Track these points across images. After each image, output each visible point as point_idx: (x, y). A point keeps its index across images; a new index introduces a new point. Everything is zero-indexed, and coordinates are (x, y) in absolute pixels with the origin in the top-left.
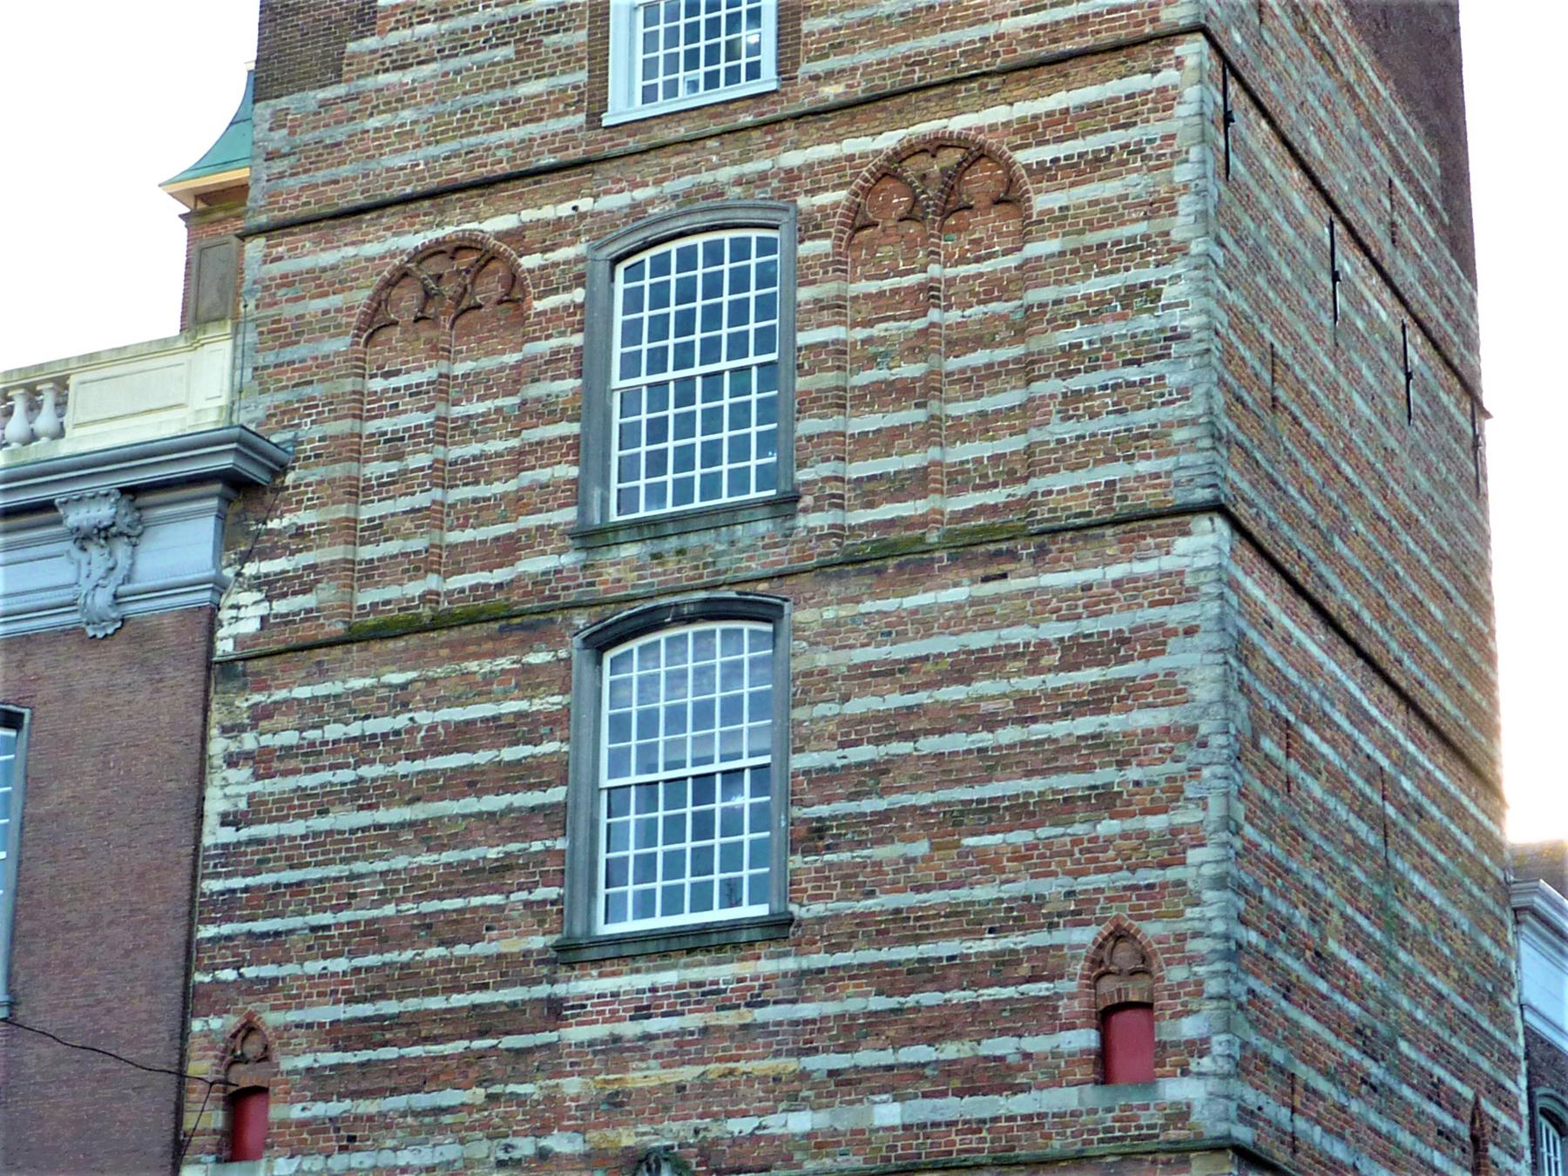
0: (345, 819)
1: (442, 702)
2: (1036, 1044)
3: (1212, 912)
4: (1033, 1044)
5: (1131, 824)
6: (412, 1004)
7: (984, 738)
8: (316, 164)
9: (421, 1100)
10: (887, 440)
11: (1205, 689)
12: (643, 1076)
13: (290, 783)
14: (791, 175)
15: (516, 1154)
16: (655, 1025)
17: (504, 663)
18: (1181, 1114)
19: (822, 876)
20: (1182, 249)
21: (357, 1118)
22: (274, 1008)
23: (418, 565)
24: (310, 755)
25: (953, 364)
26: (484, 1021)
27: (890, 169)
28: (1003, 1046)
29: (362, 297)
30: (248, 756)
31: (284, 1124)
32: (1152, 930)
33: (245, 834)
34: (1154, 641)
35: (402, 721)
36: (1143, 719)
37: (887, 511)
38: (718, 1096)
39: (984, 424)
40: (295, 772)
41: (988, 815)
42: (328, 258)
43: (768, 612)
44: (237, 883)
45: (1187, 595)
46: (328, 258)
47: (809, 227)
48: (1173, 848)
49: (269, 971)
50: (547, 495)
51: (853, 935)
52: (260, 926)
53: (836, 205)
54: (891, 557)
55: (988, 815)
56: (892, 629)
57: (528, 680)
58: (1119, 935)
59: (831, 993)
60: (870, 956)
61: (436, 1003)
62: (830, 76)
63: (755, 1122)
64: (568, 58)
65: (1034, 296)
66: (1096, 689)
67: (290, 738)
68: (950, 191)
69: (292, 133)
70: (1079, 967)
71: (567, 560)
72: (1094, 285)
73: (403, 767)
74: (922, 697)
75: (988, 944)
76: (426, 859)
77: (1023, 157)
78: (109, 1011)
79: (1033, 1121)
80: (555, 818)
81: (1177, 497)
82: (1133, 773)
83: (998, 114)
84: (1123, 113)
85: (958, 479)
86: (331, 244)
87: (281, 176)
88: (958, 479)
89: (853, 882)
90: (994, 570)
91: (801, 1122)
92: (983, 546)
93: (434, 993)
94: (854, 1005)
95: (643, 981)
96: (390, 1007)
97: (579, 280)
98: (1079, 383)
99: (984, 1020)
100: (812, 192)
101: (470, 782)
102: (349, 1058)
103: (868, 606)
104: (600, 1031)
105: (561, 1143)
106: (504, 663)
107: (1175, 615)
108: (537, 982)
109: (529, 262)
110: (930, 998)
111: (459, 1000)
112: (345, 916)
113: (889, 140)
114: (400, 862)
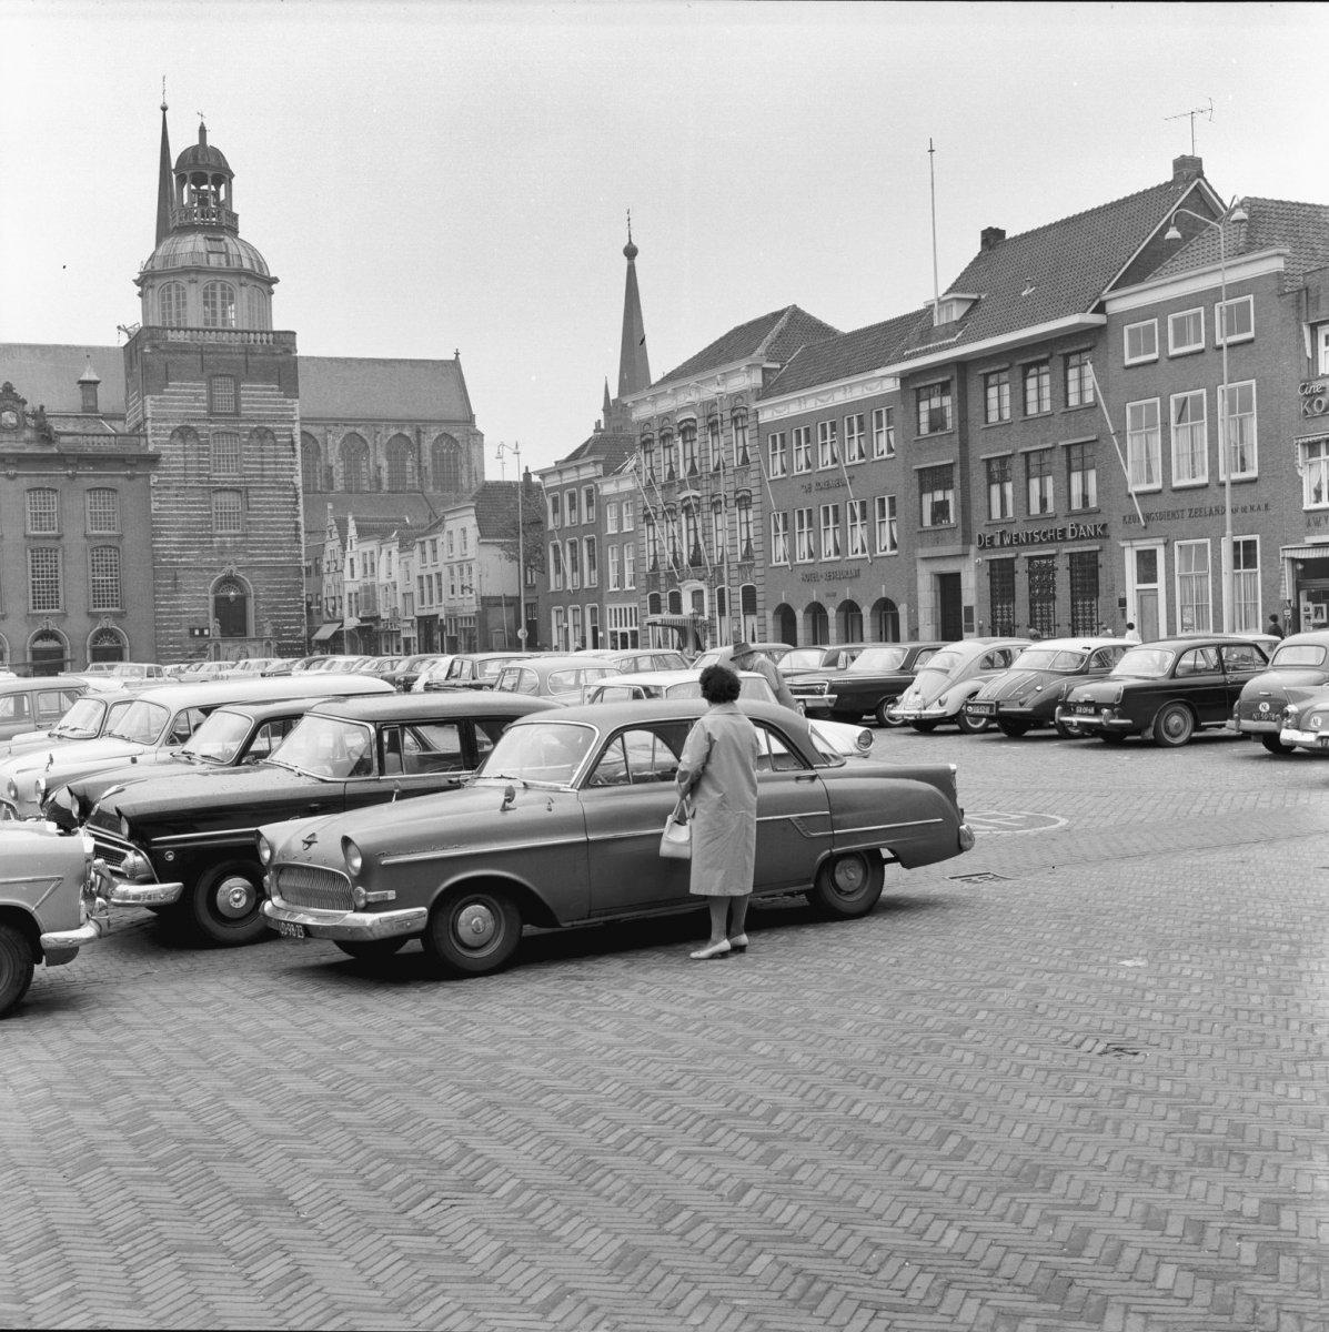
0: (175, 512)
27: (255, 430)
39: (270, 469)
47: (245, 436)
101: (195, 509)
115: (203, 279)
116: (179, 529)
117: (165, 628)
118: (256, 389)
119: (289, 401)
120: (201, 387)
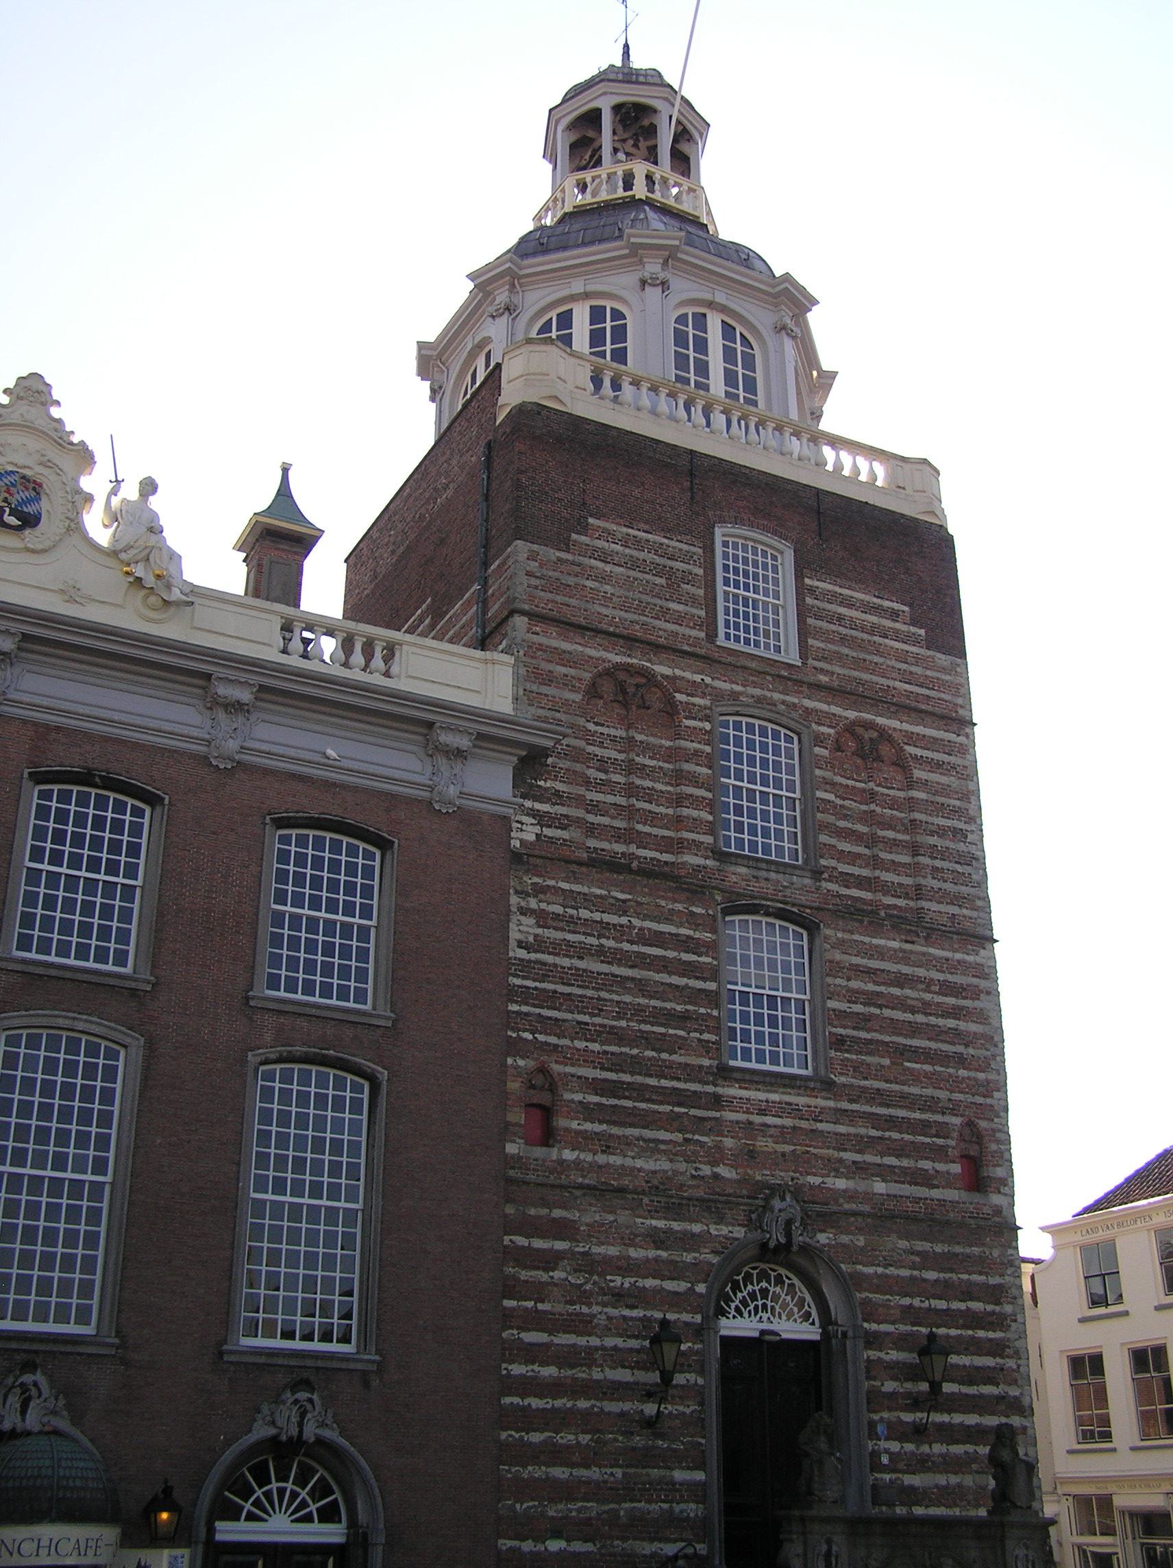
5: (972, 1074)
6: (639, 1079)
7: (909, 1016)
8: (556, 590)
9: (647, 1133)
10: (853, 858)
12: (764, 1144)
13: (559, 935)
14: (808, 711)
15: (701, 1173)
16: (770, 1120)
17: (679, 907)
21: (610, 1135)
22: (557, 1062)
23: (619, 835)
24: (572, 924)
28: (926, 1165)
30: (533, 912)
31: (567, 1130)
32: (983, 1124)
33: (533, 956)
35: (624, 920)
36: (973, 1028)
38: (802, 1162)
40: (563, 930)
42: (565, 646)
46: (565, 646)
49: (552, 1040)
51: (860, 1097)
52: (546, 1012)
53: (829, 735)
57: (692, 920)
58: (970, 1124)
59: (852, 1123)
60: (867, 1108)
61: (652, 1082)
63: (821, 1180)
64: (693, 600)
65: (917, 816)
66: (954, 1007)
67: (558, 909)
69: (541, 566)
70: (955, 1135)
73: (626, 946)
74: (882, 989)
78: (460, 1039)
80: (713, 999)
82: (971, 1051)
83: (896, 724)
85: (886, 888)
86: (566, 639)
87: (536, 587)
88: (886, 888)
89: (859, 1069)
90: (909, 938)
91: (841, 1184)
93: (651, 1076)
94: (862, 1131)
95: (762, 1096)
96: (627, 1078)
97: (707, 718)
100: (819, 724)
101: (663, 965)
102: (604, 1101)
103: (856, 937)
104: (742, 1117)
105: (723, 1171)
106: (679, 907)
108: (707, 1083)
110: (895, 1135)
111: (664, 1083)
112: (597, 1020)
113: (851, 714)
114: (628, 999)
115: (684, 288)
118: (847, 603)
119: (942, 659)
120: (687, 558)
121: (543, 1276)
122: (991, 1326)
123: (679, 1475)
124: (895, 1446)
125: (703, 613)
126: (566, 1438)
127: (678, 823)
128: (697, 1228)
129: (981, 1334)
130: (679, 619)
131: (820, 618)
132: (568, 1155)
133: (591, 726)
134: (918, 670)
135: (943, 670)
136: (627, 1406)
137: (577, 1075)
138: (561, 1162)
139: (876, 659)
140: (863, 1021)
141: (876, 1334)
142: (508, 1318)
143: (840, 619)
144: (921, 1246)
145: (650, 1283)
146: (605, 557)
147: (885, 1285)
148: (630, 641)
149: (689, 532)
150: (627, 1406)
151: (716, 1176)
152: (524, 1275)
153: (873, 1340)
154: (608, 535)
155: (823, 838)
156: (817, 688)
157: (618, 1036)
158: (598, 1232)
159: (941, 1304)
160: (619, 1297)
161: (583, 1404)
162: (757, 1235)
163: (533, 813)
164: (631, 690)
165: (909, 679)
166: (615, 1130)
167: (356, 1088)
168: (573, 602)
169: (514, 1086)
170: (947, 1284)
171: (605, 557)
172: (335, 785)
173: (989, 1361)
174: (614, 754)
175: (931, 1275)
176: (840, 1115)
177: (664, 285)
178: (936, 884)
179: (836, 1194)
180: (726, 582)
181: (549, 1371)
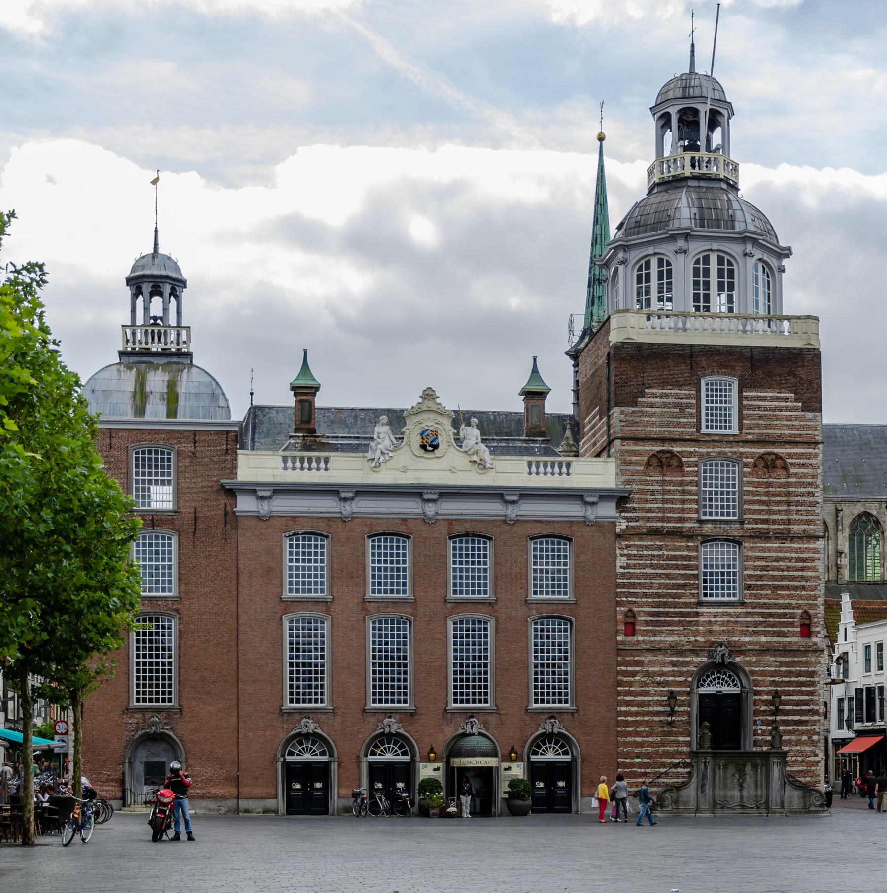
0: (649, 571)
1: (670, 550)
2: (791, 629)
3: (821, 610)
4: (790, 629)
6: (667, 610)
7: (781, 573)
8: (632, 425)
10: (760, 512)
11: (821, 571)
12: (716, 628)
13: (636, 562)
14: (741, 453)
16: (718, 619)
17: (683, 544)
18: (815, 644)
19: (750, 595)
20: (818, 486)
23: (661, 520)
24: (641, 557)
25: (773, 499)
26: (682, 614)
27: (761, 457)
29: (645, 459)
32: (811, 612)
33: (626, 571)
34: (812, 560)
35: (661, 553)
36: (810, 574)
37: (760, 526)
39: (779, 512)
41: (782, 587)
43: (740, 544)
44: (625, 581)
45: (818, 552)
47: (746, 465)
48: (815, 598)
49: (634, 600)
50: (690, 511)
52: (631, 590)
54: (763, 536)
55: (782, 587)
56: (763, 550)
57: (688, 548)
59: (752, 617)
60: (760, 611)
61: (672, 610)
62: (749, 434)
64: (691, 415)
65: (790, 489)
67: (635, 552)
68: (770, 464)
71: (696, 525)
72: (802, 490)
73: (662, 562)
75: (782, 611)
76: (668, 581)
77: (788, 460)
79: (790, 643)
80: (696, 577)
81: (817, 534)
82: (808, 583)
83: (784, 450)
84: (808, 456)
85: (774, 522)
88: (774, 522)
89: (756, 596)
91: (747, 639)
92: (783, 536)
94: (757, 619)
95: (715, 610)
96: (662, 610)
97: (696, 466)
98: (799, 508)
99: (781, 624)
101: (677, 567)
104: (707, 619)
105: (699, 638)
106: (683, 544)
107: (816, 556)
109: (684, 459)
110: (771, 619)
111: (677, 610)
113: (762, 451)
114: (662, 581)
116: (652, 595)
117: (630, 734)
118: (763, 399)
119: (809, 415)
120: (689, 397)
121: (632, 679)
122: (808, 686)
123: (680, 739)
124: (764, 728)
125: (695, 420)
126: (641, 729)
127: (683, 510)
128: (688, 659)
129: (804, 688)
130: (684, 425)
131: (748, 409)
132: (640, 638)
133: (648, 478)
134: (796, 423)
135: (810, 420)
136: (662, 718)
137: (643, 611)
138: (638, 641)
139: (776, 422)
140: (760, 578)
141: (758, 691)
142: (619, 693)
143: (759, 408)
144: (779, 659)
145: (670, 679)
146: (652, 406)
147: (763, 674)
148: (663, 440)
149: (690, 384)
150: (662, 718)
151: (696, 641)
152: (625, 679)
153: (757, 693)
154: (654, 395)
155: (746, 507)
156: (746, 442)
157: (659, 595)
158: (650, 663)
159: (788, 679)
160: (659, 684)
161: (646, 718)
162: (711, 660)
163: (625, 518)
164: (664, 460)
165: (791, 428)
166: (657, 628)
167: (566, 624)
168: (639, 428)
169: (620, 617)
170: (790, 672)
171: (652, 406)
172: (550, 522)
173: (807, 698)
174: (657, 487)
175: (784, 669)
176: (747, 614)
177: (685, 252)
178: (797, 517)
179: (744, 644)
180: (707, 402)
181: (635, 709)
